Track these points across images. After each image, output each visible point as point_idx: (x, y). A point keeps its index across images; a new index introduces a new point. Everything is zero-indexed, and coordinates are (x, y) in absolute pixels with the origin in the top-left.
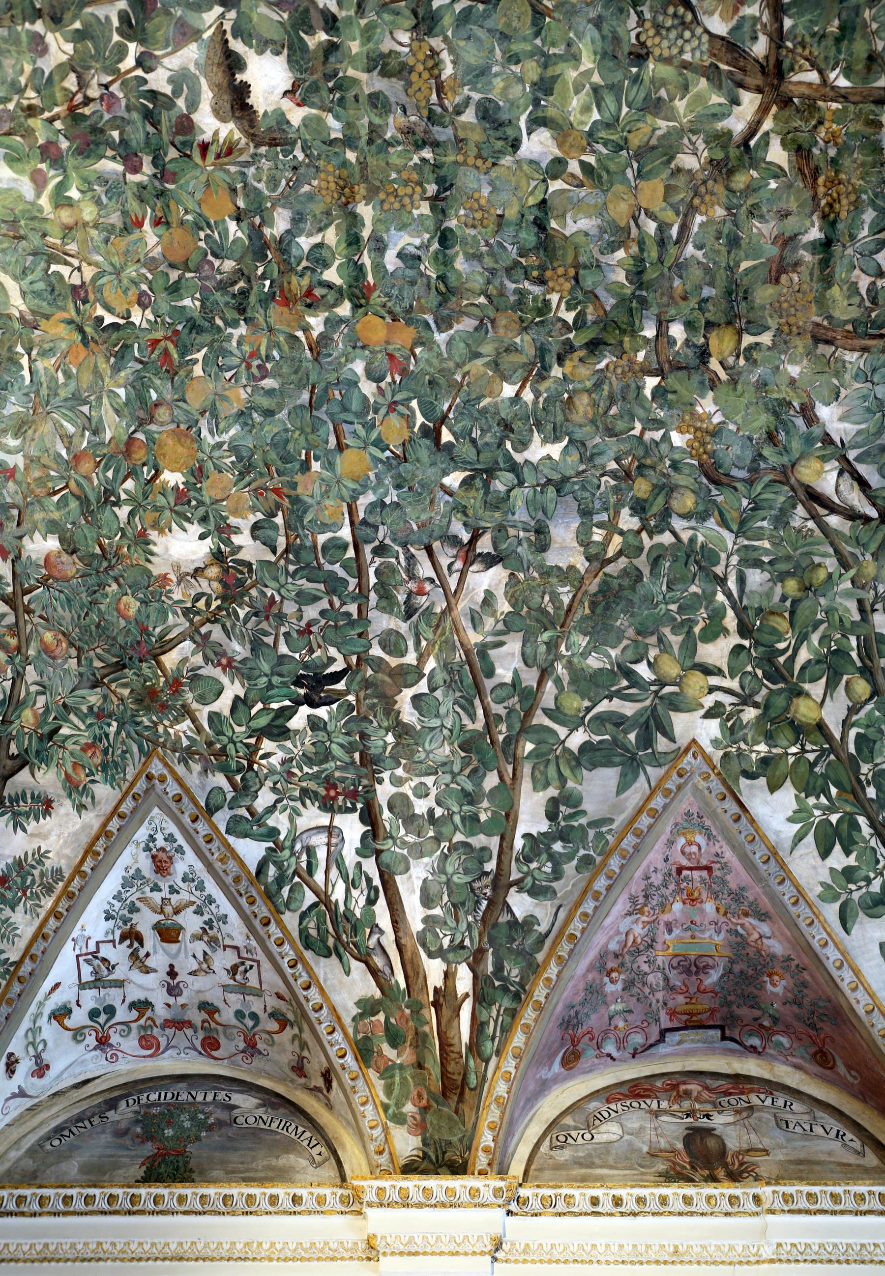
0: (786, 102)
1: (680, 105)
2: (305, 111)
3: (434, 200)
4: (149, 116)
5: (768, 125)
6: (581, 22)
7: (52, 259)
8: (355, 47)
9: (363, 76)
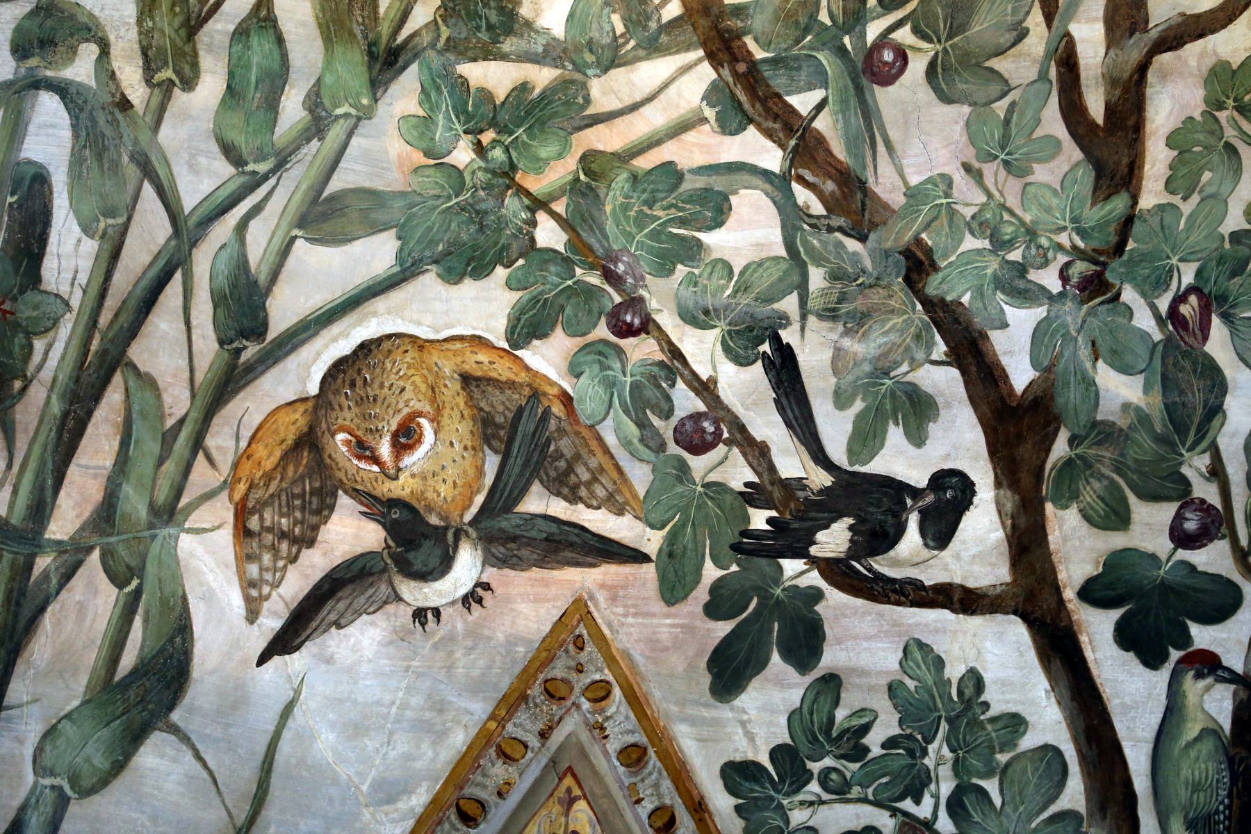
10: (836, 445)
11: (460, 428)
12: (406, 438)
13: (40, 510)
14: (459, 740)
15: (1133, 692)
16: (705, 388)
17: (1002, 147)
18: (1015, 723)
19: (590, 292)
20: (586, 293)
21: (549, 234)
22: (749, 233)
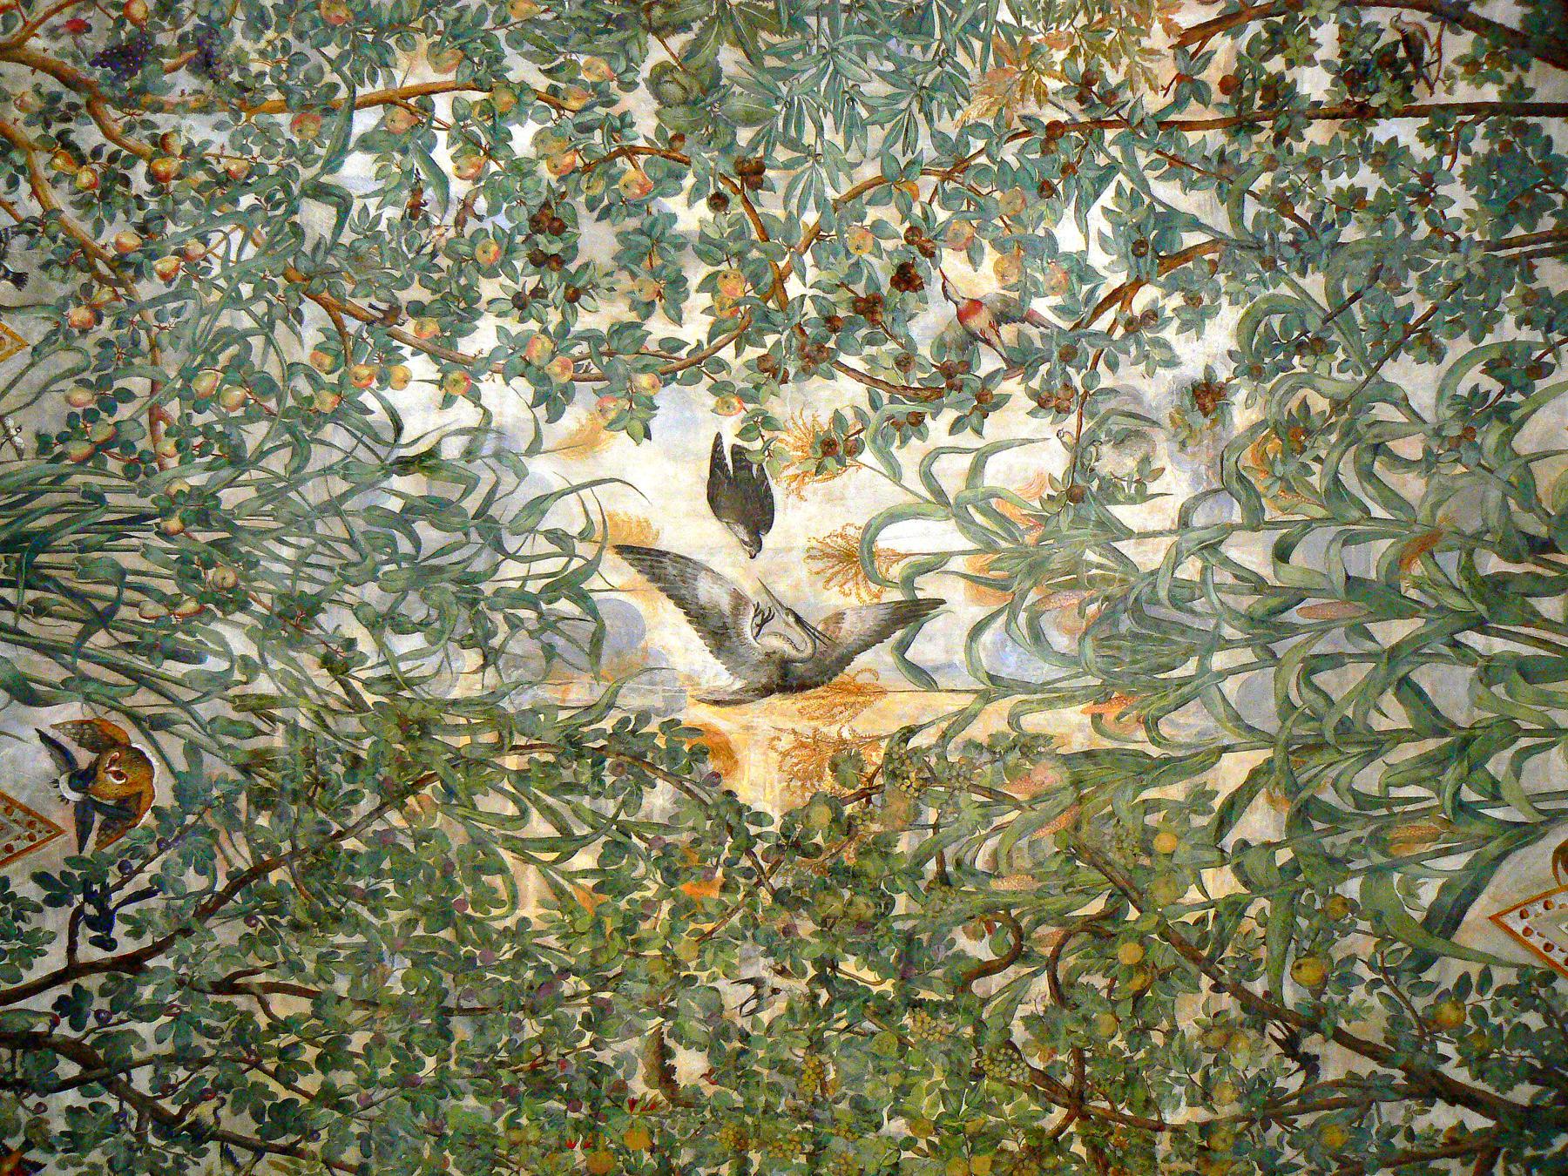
0: (1085, 1117)
1: (1007, 1108)
2: (717, 1087)
3: (810, 1156)
4: (592, 1078)
5: (1072, 1128)
6: (934, 1051)
7: (496, 1163)
8: (761, 1054)
9: (766, 1072)
10: (124, 910)
11: (122, 793)
12: (118, 775)
13: (87, 657)
14: (12, 794)
15: (44, 1002)
16: (140, 870)
17: (226, 954)
18: (29, 967)
19: (171, 831)
20: (170, 830)
21: (190, 819)
22: (194, 882)
